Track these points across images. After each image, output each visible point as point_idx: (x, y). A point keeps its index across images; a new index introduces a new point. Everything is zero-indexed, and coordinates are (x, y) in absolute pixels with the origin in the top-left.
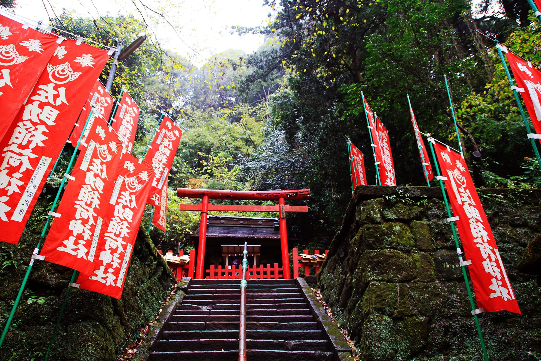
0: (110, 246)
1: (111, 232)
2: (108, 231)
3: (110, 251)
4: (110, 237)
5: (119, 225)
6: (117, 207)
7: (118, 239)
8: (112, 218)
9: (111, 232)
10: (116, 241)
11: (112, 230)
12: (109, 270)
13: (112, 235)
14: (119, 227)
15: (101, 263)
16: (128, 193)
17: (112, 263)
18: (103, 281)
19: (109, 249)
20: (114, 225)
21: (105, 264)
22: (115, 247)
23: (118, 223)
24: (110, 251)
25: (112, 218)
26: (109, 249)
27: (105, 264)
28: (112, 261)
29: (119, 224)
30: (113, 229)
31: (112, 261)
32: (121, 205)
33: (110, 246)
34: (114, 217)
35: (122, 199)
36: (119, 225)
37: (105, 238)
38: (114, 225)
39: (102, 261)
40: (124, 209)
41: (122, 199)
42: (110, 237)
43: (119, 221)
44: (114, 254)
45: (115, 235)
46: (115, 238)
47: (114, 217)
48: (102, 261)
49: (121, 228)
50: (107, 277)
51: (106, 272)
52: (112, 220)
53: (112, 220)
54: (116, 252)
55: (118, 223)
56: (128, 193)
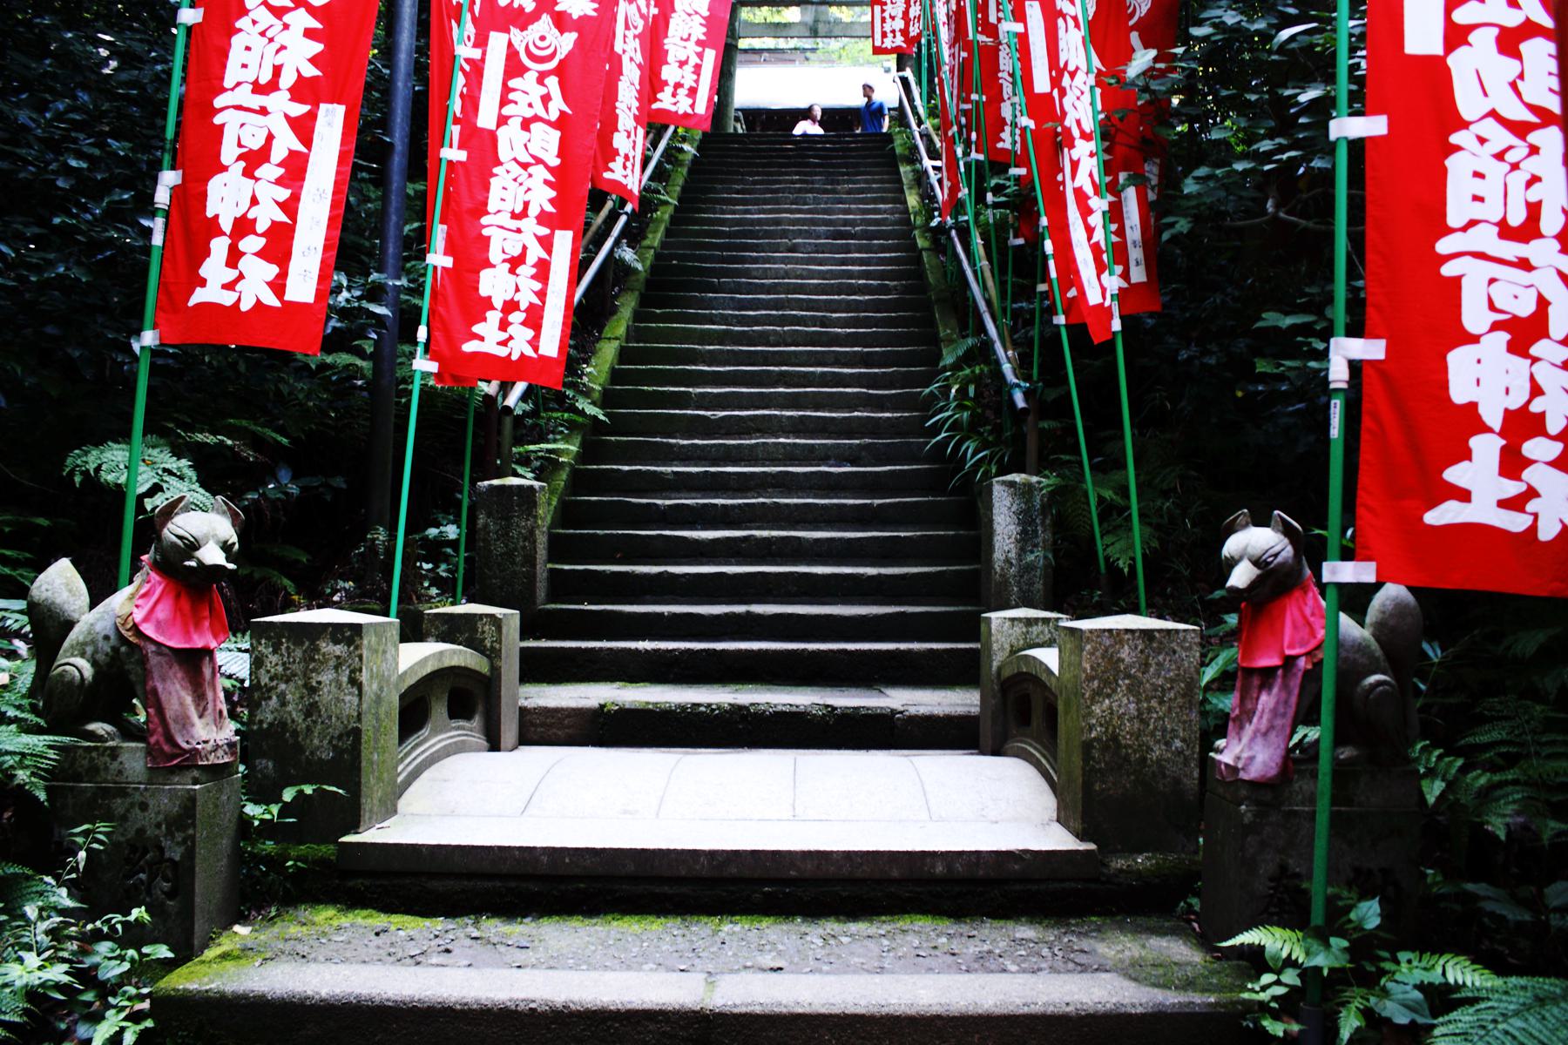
0: (1492, 307)
1: (1472, 223)
2: (1454, 218)
3: (1503, 337)
5: (1515, 167)
6: (1461, 64)
7: (1535, 250)
8: (1455, 139)
9: (1472, 223)
10: (1524, 265)
11: (1477, 211)
12: (1534, 448)
14: (1520, 177)
15: (1470, 419)
17: (1535, 407)
18: (1515, 522)
19: (1496, 326)
21: (1493, 418)
22: (1526, 308)
23: (1500, 156)
24: (1503, 337)
25: (1455, 139)
26: (1496, 326)
27: (1493, 418)
28: (1536, 390)
29: (1511, 157)
30: (1478, 199)
31: (1536, 390)
32: (1484, 40)
33: (1492, 307)
34: (500, 163)
36: (1515, 167)
37: (1448, 270)
38: (1478, 175)
39: (1473, 406)
40: (1517, 56)
43: (1501, 138)
44: (1535, 350)
45: (1506, 231)
46: (1512, 250)
47: (500, 163)
48: (1473, 406)
49: (1534, 180)
50: (1531, 493)
51: (1512, 464)
52: (1458, 148)
53: (1458, 148)
54: (1543, 333)
55: (1500, 156)
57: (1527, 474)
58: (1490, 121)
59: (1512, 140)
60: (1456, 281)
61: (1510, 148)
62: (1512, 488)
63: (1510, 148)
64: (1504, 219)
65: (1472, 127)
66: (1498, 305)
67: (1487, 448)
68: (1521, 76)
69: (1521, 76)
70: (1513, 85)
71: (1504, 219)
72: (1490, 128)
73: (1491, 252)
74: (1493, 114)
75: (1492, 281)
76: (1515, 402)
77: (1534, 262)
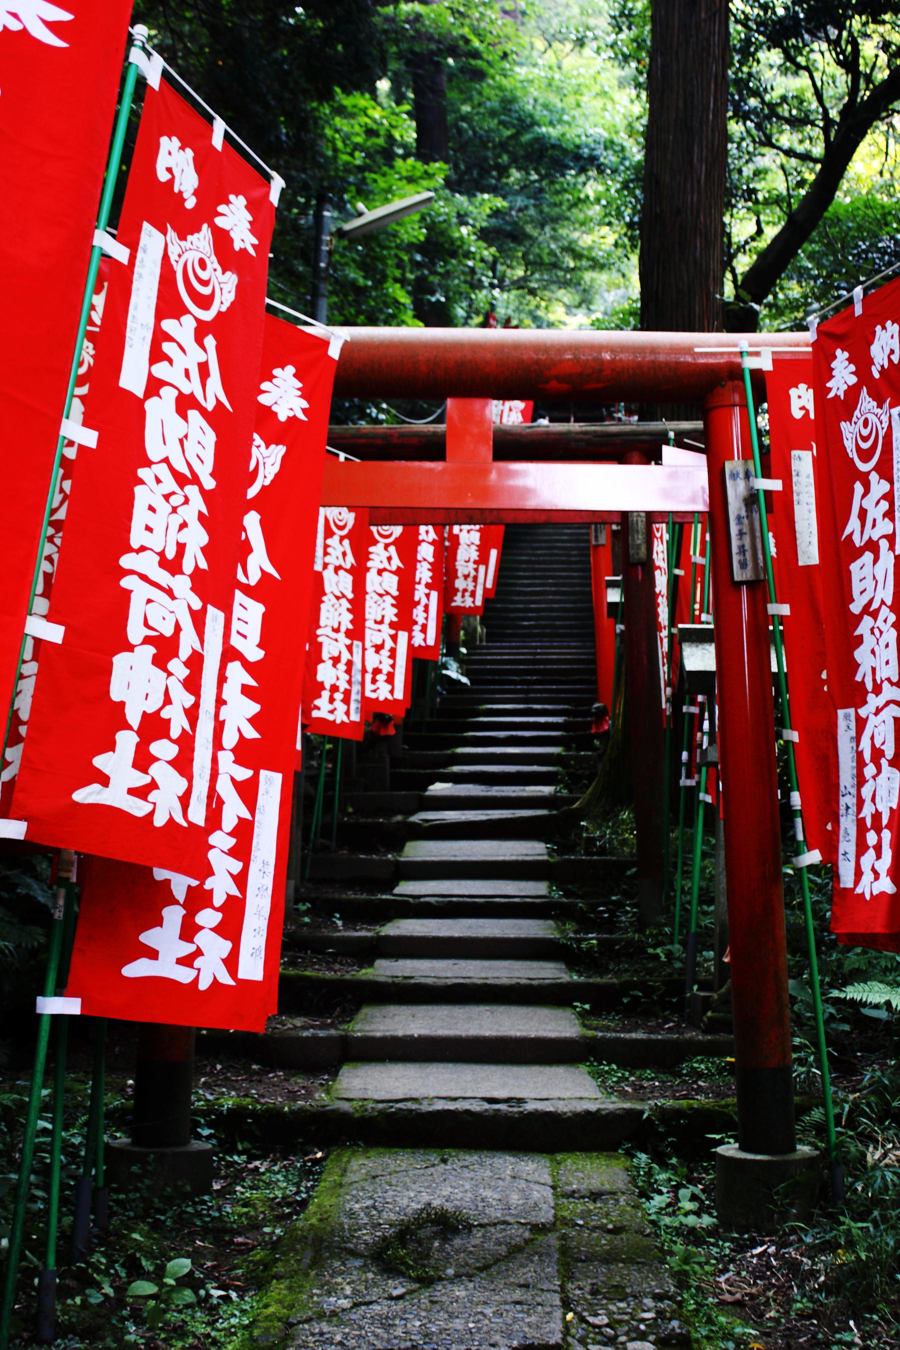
0: (146, 624)
1: (143, 549)
3: (151, 650)
4: (144, 578)
9: (143, 549)
13: (147, 563)
16: (189, 323)
17: (164, 714)
19: (147, 640)
20: (151, 509)
21: (134, 719)
24: (151, 650)
26: (147, 640)
28: (167, 701)
33: (146, 624)
35: (170, 361)
38: (151, 509)
39: (122, 704)
41: (170, 361)
42: (144, 578)
48: (122, 704)
49: (184, 525)
52: (142, 482)
53: (142, 482)
55: (167, 497)
56: (189, 323)
57: (154, 769)
58: (164, 465)
59: (177, 489)
60: (127, 593)
61: (173, 493)
62: (144, 780)
63: (173, 493)
64: (163, 551)
65: (153, 466)
66: (151, 623)
67: (127, 741)
68: (186, 436)
69: (186, 436)
70: (181, 441)
71: (163, 551)
72: (162, 471)
73: (152, 577)
74: (166, 460)
75: (149, 601)
76: (151, 709)
77: (176, 594)
